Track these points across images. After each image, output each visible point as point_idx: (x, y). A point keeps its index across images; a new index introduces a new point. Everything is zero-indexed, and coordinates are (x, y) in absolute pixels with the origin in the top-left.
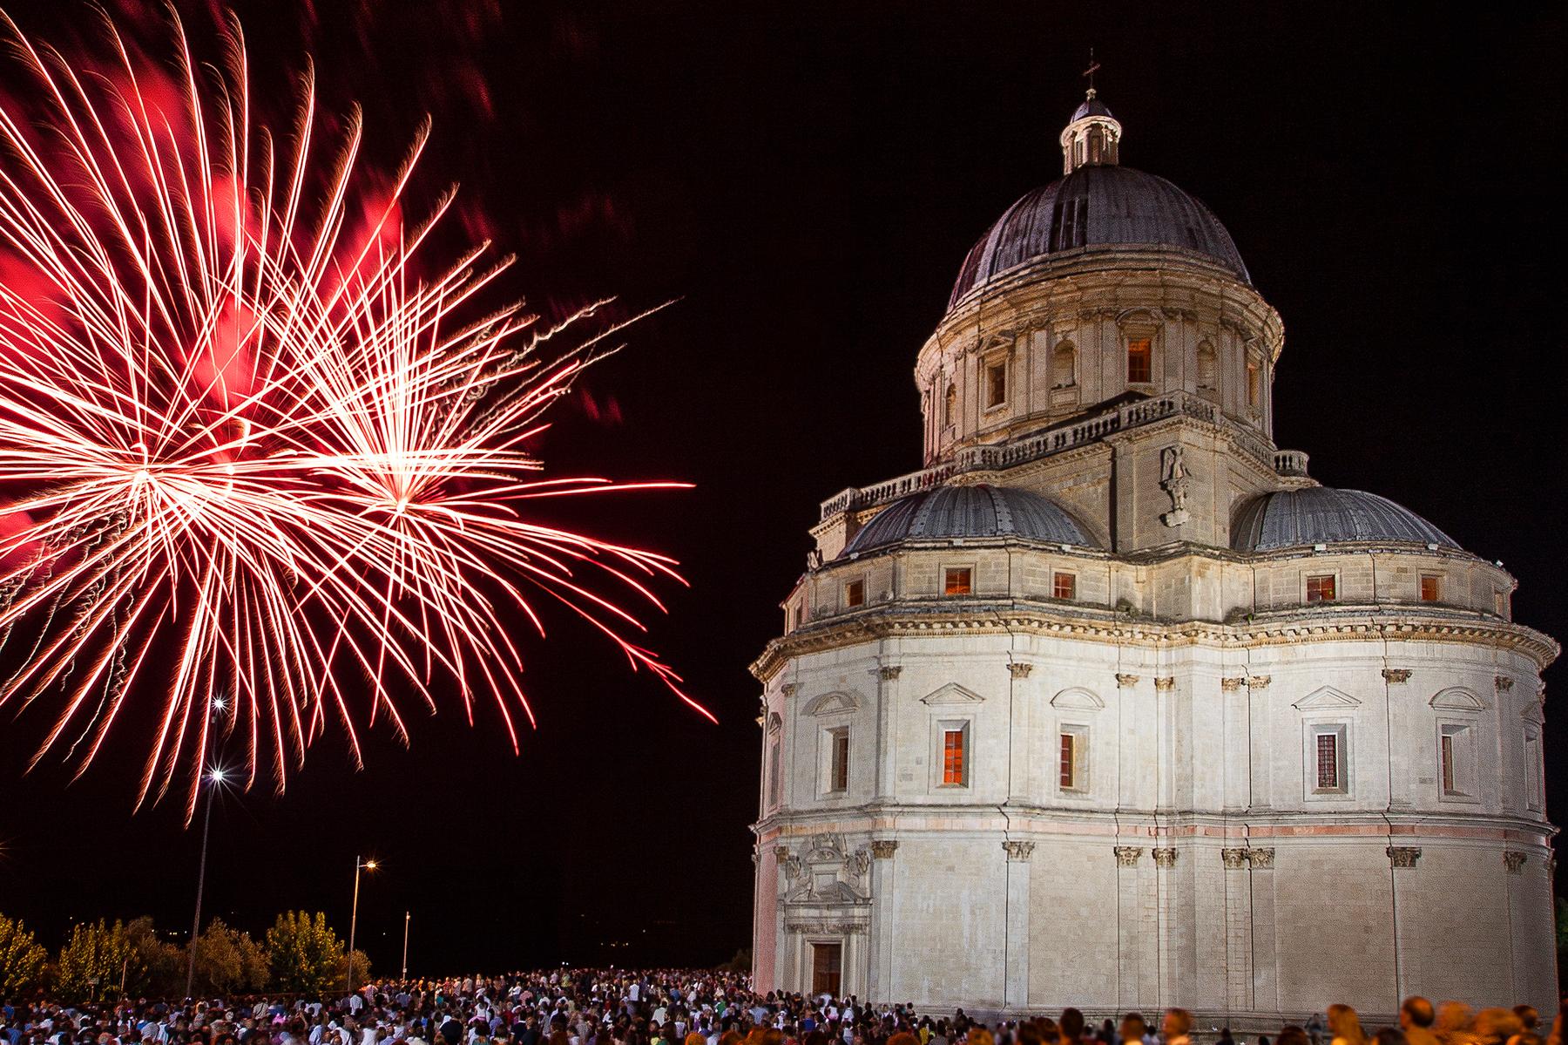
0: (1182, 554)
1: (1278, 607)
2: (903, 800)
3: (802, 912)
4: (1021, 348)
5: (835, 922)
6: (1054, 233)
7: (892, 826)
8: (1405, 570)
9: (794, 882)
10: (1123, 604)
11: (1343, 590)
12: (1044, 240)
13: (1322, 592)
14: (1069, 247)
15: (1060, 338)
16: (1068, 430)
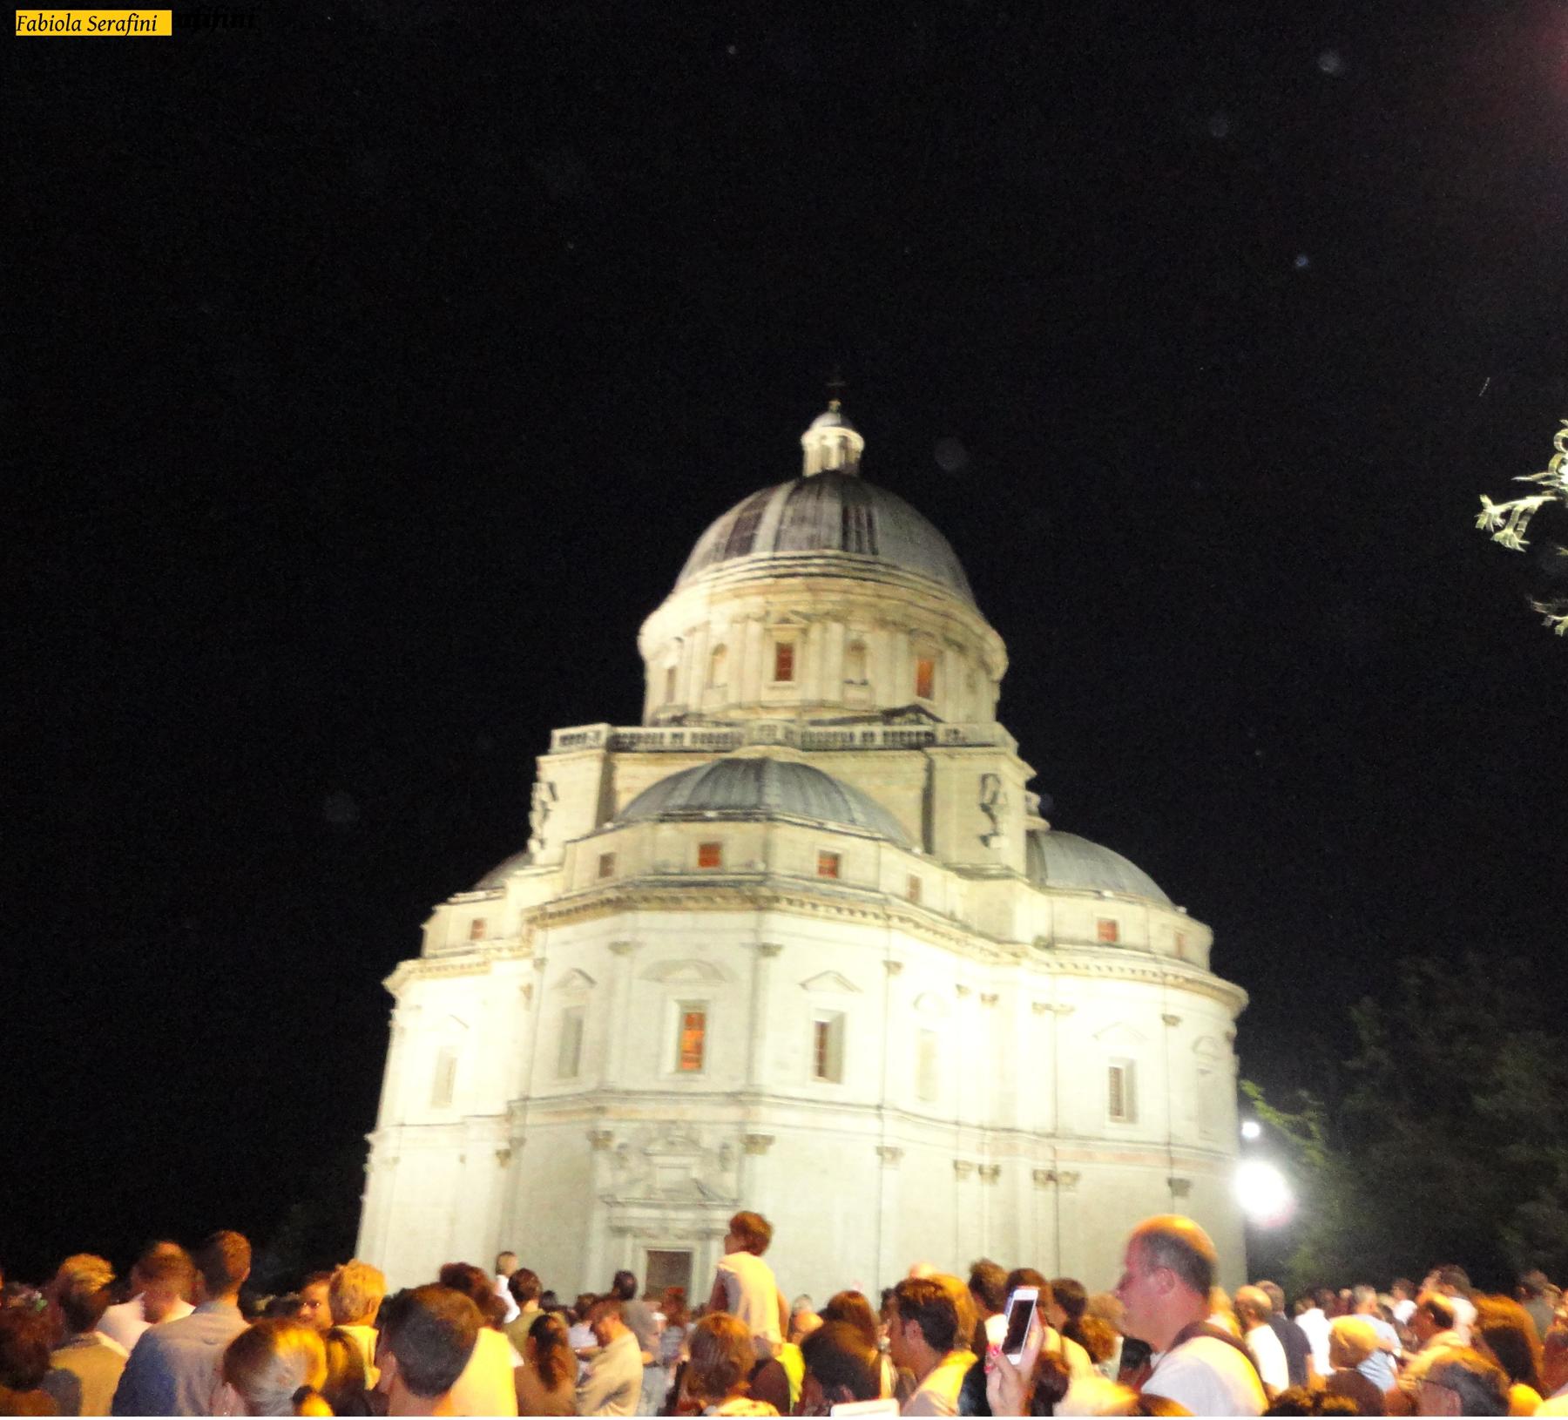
0: (1008, 877)
1: (1073, 942)
2: (779, 1091)
3: (635, 1212)
4: (815, 632)
5: (682, 1225)
6: (845, 534)
7: (767, 1120)
8: (1164, 926)
9: (622, 1177)
10: (952, 917)
11: (1127, 934)
12: (836, 538)
13: (1110, 935)
14: (860, 551)
15: (853, 636)
16: (878, 729)
